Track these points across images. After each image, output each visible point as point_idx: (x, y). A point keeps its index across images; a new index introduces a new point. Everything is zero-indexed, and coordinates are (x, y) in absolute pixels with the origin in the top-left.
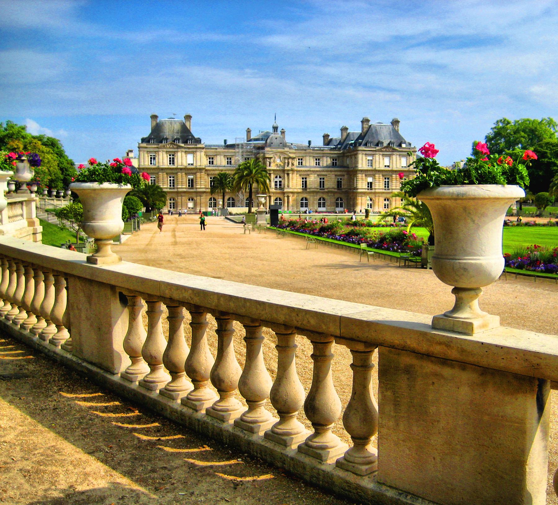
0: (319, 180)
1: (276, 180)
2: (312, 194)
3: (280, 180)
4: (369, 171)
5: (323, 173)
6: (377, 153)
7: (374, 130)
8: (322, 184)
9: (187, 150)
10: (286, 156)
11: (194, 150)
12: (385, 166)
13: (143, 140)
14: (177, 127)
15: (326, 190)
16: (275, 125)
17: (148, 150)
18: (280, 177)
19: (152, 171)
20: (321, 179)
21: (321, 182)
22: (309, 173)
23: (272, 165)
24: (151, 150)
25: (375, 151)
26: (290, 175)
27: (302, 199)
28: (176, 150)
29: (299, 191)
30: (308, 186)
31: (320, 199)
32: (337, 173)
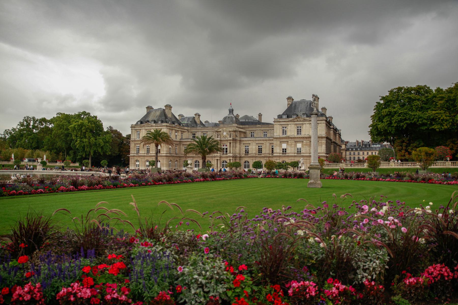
0: (257, 147)
1: (223, 147)
2: (252, 158)
3: (226, 147)
4: (283, 138)
5: (261, 142)
6: (290, 123)
7: (293, 105)
8: (260, 150)
10: (230, 130)
14: (158, 113)
15: (262, 155)
17: (136, 128)
18: (226, 146)
19: (137, 142)
22: (249, 142)
23: (219, 137)
24: (138, 128)
25: (288, 122)
29: (243, 155)
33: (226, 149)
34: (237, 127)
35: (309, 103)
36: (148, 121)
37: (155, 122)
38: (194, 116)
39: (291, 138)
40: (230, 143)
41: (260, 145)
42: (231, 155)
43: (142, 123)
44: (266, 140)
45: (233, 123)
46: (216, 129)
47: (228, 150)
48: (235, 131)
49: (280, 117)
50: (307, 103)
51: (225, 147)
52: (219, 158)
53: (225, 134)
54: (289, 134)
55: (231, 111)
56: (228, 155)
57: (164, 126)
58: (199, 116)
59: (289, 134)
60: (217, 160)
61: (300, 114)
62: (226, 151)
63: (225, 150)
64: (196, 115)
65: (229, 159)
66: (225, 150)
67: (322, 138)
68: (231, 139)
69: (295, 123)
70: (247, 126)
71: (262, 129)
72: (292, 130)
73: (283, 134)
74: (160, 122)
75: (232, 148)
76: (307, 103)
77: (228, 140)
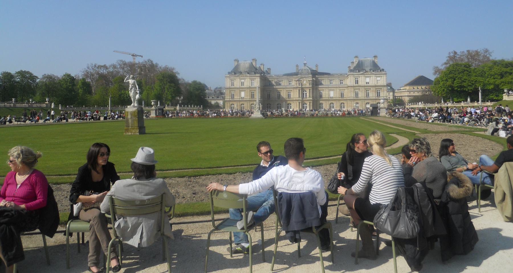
12: (367, 83)
13: (229, 73)
16: (305, 62)
31: (331, 104)
36: (241, 73)
37: (248, 73)
39: (362, 86)
42: (311, 99)
43: (235, 74)
44: (337, 87)
45: (309, 74)
46: (297, 79)
47: (308, 95)
48: (313, 80)
53: (305, 82)
56: (308, 99)
59: (360, 83)
61: (368, 69)
64: (261, 65)
67: (384, 86)
68: (311, 86)
72: (363, 80)
74: (253, 73)
77: (308, 88)
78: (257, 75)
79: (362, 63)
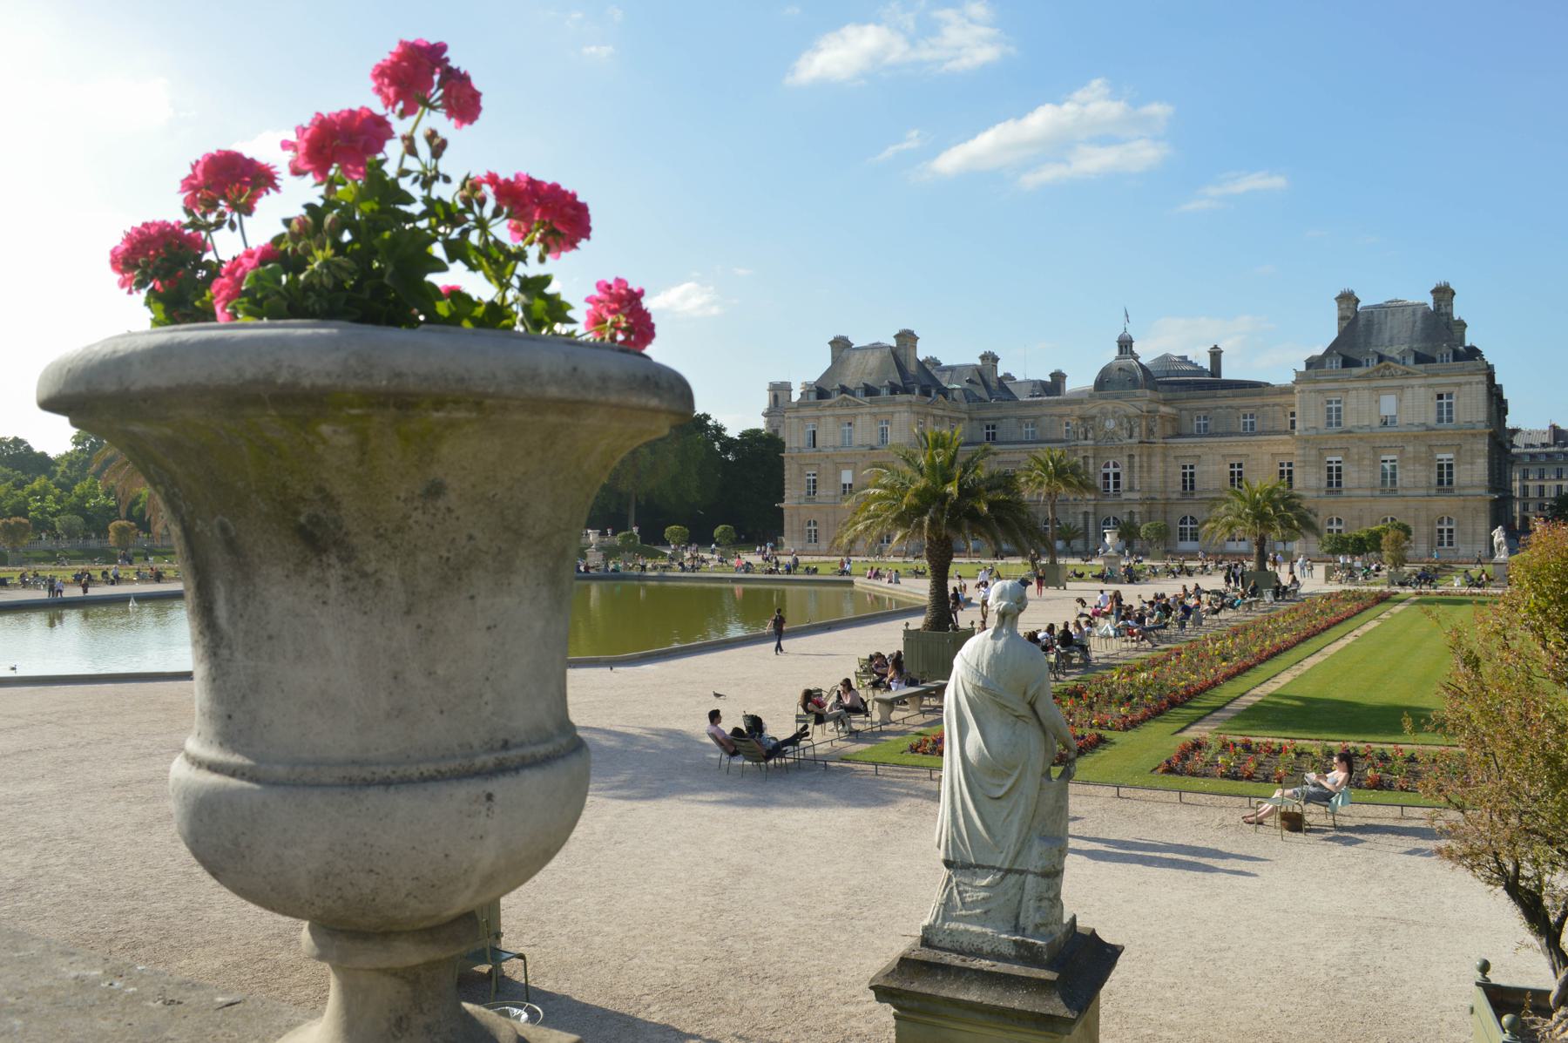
0: (1228, 469)
6: (1356, 384)
7: (1361, 322)
8: (1236, 477)
9: (875, 410)
10: (1132, 411)
11: (891, 409)
18: (1115, 466)
20: (1232, 466)
21: (1232, 473)
26: (1137, 459)
27: (1183, 521)
28: (854, 411)
29: (1175, 496)
30: (1197, 487)
32: (1275, 449)
33: (1117, 476)
34: (1151, 401)
35: (1419, 314)
36: (844, 390)
38: (979, 363)
40: (1131, 456)
41: (1236, 461)
42: (1136, 496)
47: (1124, 480)
49: (1311, 363)
50: (1414, 314)
51: (1111, 470)
52: (1090, 509)
54: (1349, 421)
55: (1125, 345)
56: (1124, 496)
57: (902, 404)
58: (996, 359)
59: (1349, 421)
60: (1086, 514)
62: (1117, 485)
63: (1111, 481)
64: (983, 358)
65: (1126, 510)
66: (1111, 481)
69: (1374, 384)
70: (1184, 394)
71: (1237, 402)
73: (1330, 424)
75: (1136, 475)
76: (1414, 314)
78: (900, 397)
79: (1369, 323)
